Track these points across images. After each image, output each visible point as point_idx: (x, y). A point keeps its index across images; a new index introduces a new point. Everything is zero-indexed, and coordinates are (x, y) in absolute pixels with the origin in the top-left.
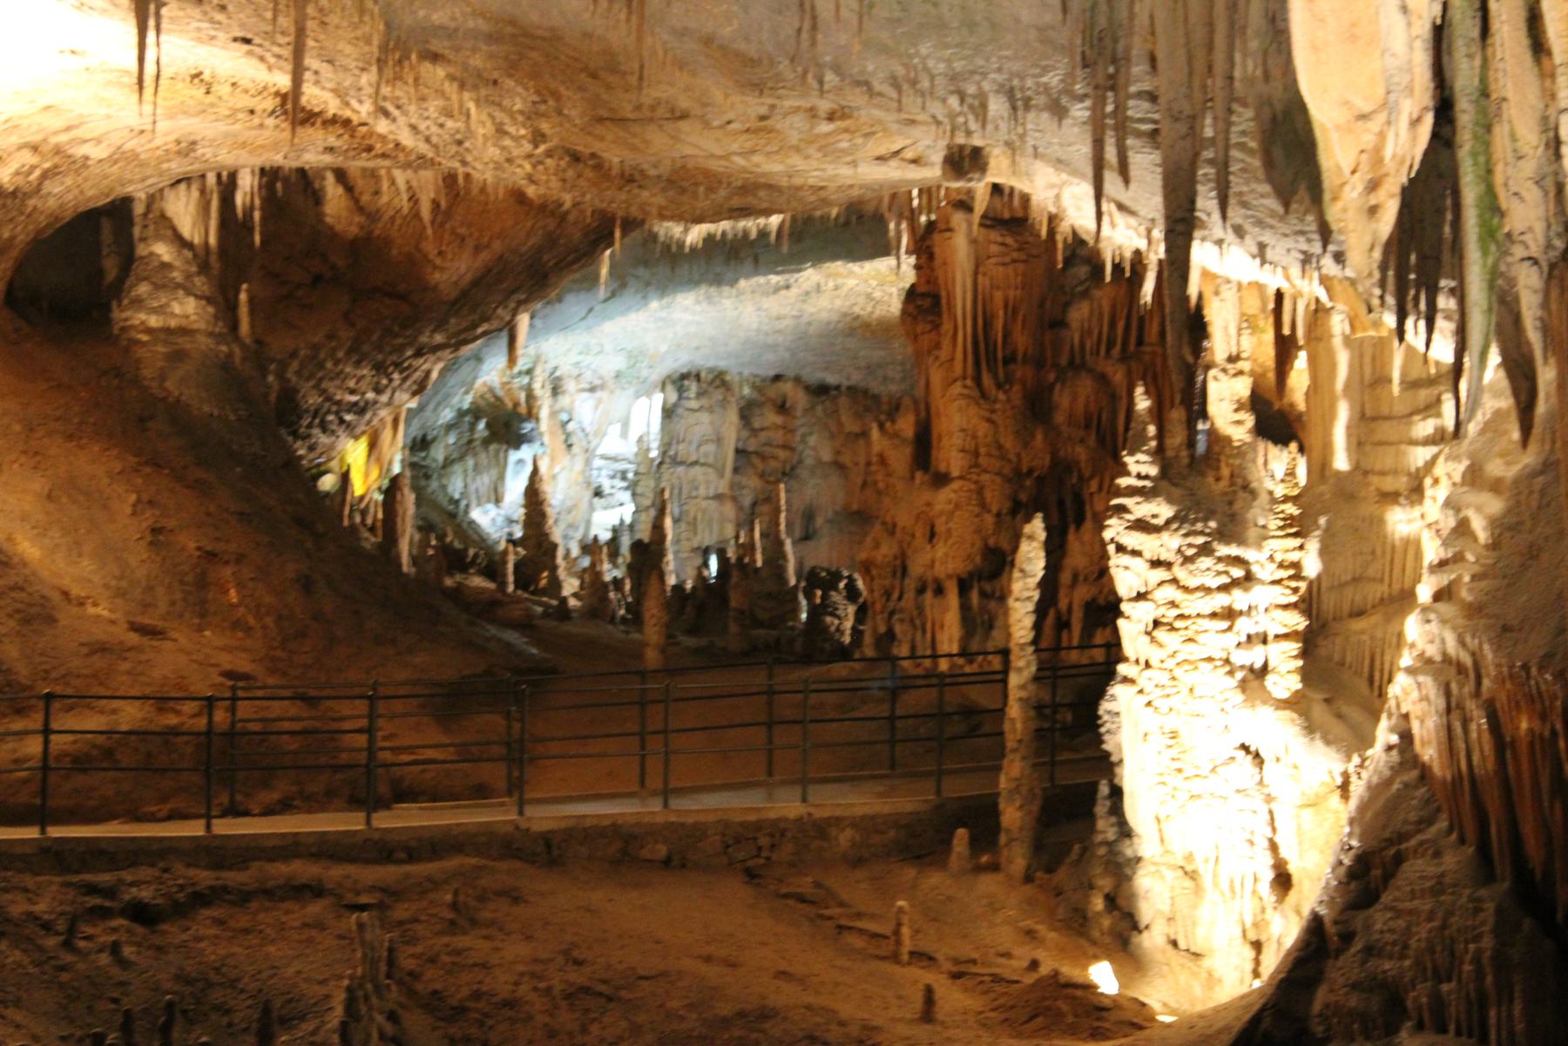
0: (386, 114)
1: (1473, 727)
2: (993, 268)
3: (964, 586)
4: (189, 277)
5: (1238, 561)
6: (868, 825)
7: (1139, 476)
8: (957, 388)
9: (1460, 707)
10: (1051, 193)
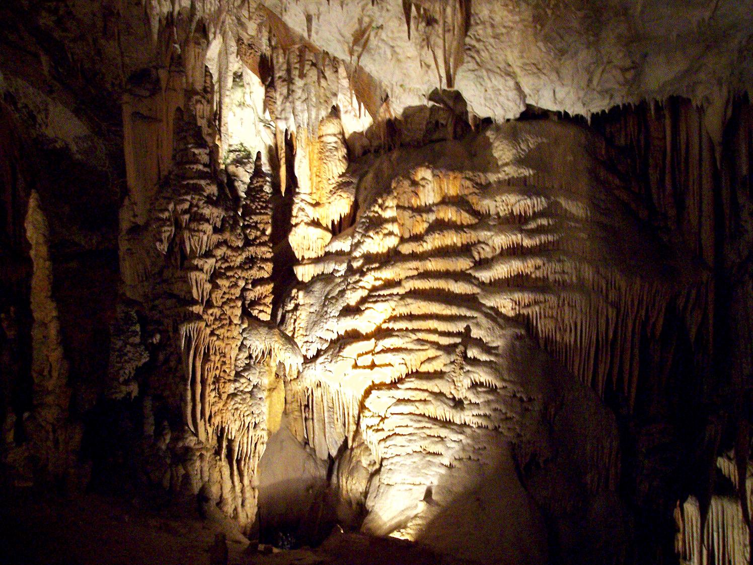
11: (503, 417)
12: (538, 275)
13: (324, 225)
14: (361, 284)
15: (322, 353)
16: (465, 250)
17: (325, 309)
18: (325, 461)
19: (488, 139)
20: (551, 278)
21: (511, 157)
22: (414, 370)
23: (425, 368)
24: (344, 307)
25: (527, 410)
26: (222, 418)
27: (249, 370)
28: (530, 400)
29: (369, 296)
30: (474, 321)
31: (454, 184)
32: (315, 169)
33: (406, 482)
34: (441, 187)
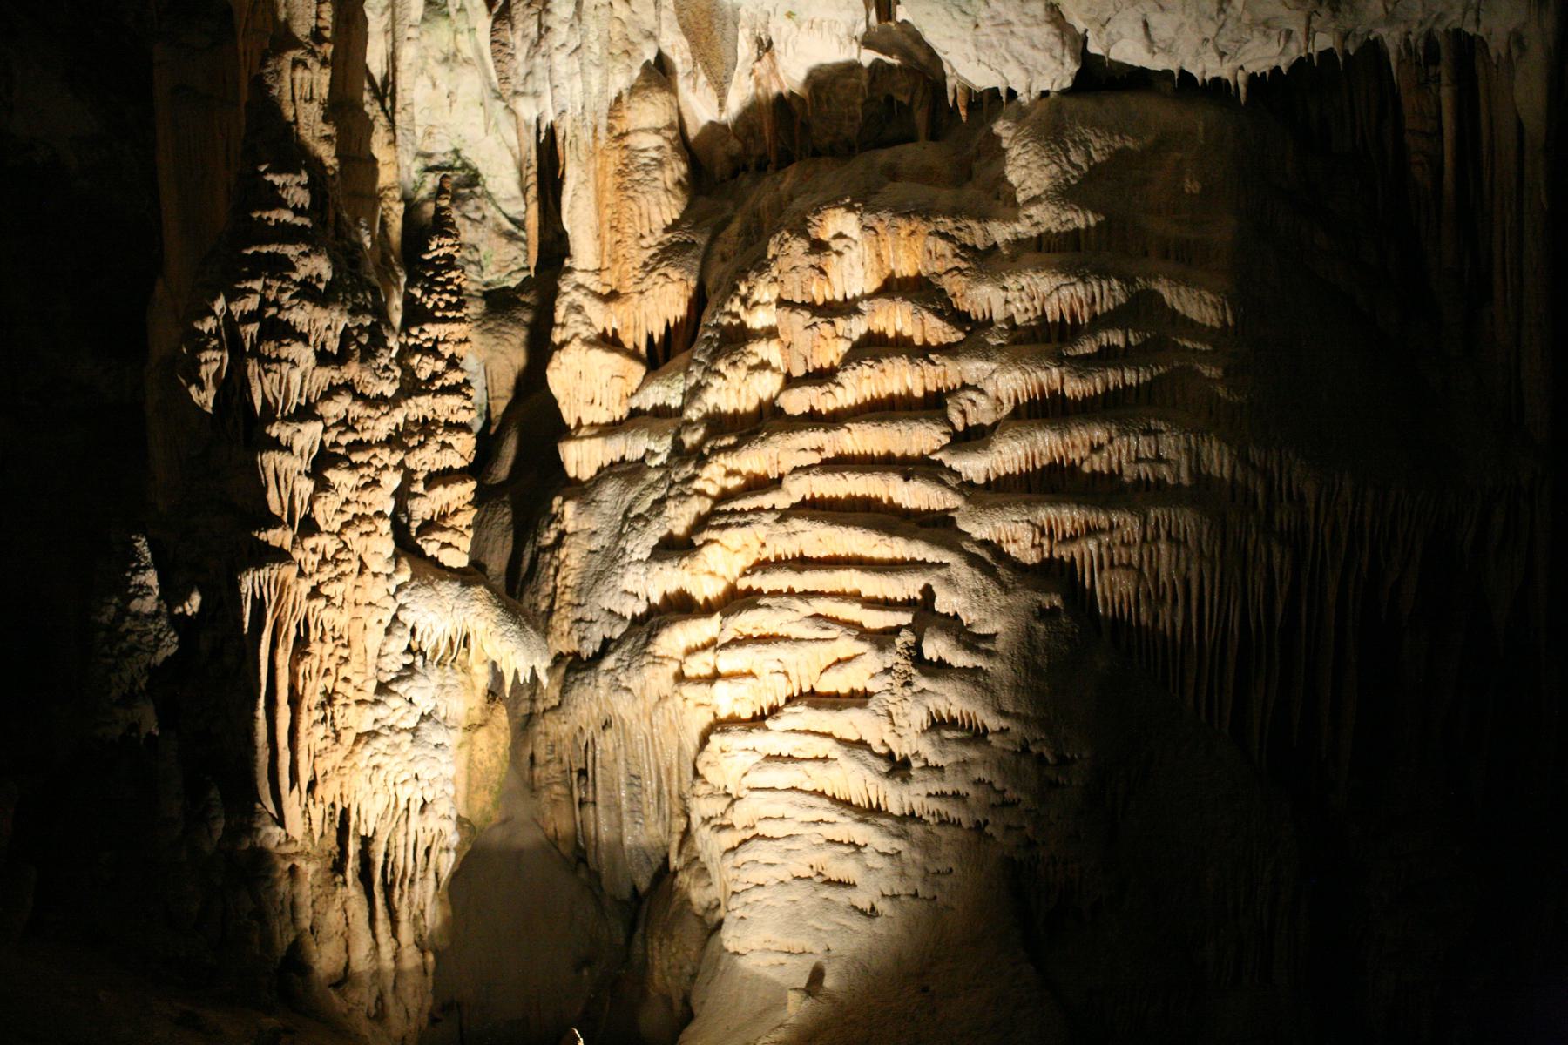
7: (298, 211)
11: (994, 799)
12: (1097, 467)
13: (630, 346)
14: (698, 485)
15: (612, 647)
16: (931, 406)
17: (622, 543)
18: (623, 902)
19: (998, 138)
20: (1129, 473)
21: (1046, 182)
22: (806, 689)
23: (827, 684)
24: (661, 540)
25: (1054, 785)
26: (342, 786)
27: (410, 677)
28: (1062, 761)
29: (713, 513)
30: (943, 573)
31: (908, 249)
32: (609, 211)
33: (773, 947)
34: (879, 255)
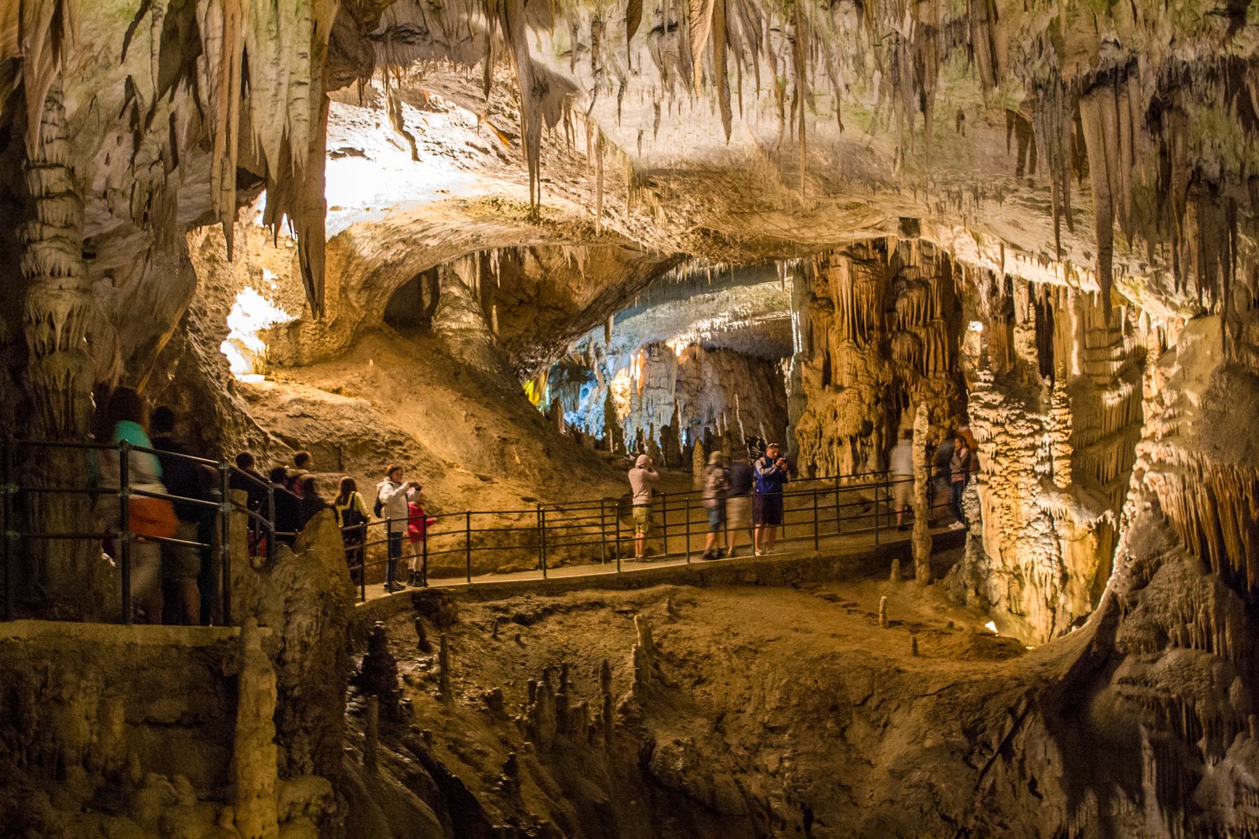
0: (609, 215)
1: (1199, 497)
2: (861, 283)
3: (853, 440)
4: (469, 303)
5: (1037, 421)
6: (847, 559)
7: (985, 381)
8: (845, 343)
9: (1191, 487)
10: (947, 244)
